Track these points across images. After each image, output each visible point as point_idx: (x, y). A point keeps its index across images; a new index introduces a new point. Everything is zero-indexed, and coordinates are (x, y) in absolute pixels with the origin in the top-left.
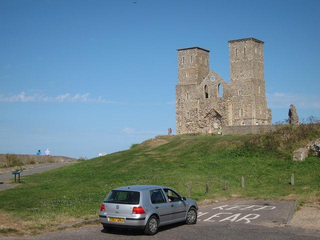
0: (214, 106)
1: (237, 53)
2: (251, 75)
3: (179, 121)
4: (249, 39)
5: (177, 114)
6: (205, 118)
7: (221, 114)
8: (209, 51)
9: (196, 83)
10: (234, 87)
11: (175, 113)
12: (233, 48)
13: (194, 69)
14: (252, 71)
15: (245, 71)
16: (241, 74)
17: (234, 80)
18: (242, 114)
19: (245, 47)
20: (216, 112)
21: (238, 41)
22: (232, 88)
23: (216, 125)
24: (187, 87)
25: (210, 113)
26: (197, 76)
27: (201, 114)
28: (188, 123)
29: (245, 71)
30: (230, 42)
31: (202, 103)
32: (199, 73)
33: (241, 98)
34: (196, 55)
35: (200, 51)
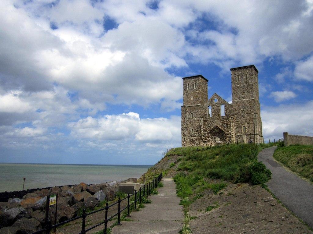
1: (238, 78)
2: (253, 97)
6: (208, 133)
7: (224, 130)
8: (207, 81)
9: (200, 104)
10: (236, 107)
13: (199, 93)
17: (236, 101)
18: (245, 130)
19: (247, 73)
22: (234, 108)
23: (218, 140)
24: (192, 108)
25: (213, 130)
26: (200, 98)
27: (205, 130)
28: (193, 138)
29: (247, 94)
31: (205, 121)
32: (202, 97)
33: (243, 116)
34: (199, 81)
35: (203, 80)
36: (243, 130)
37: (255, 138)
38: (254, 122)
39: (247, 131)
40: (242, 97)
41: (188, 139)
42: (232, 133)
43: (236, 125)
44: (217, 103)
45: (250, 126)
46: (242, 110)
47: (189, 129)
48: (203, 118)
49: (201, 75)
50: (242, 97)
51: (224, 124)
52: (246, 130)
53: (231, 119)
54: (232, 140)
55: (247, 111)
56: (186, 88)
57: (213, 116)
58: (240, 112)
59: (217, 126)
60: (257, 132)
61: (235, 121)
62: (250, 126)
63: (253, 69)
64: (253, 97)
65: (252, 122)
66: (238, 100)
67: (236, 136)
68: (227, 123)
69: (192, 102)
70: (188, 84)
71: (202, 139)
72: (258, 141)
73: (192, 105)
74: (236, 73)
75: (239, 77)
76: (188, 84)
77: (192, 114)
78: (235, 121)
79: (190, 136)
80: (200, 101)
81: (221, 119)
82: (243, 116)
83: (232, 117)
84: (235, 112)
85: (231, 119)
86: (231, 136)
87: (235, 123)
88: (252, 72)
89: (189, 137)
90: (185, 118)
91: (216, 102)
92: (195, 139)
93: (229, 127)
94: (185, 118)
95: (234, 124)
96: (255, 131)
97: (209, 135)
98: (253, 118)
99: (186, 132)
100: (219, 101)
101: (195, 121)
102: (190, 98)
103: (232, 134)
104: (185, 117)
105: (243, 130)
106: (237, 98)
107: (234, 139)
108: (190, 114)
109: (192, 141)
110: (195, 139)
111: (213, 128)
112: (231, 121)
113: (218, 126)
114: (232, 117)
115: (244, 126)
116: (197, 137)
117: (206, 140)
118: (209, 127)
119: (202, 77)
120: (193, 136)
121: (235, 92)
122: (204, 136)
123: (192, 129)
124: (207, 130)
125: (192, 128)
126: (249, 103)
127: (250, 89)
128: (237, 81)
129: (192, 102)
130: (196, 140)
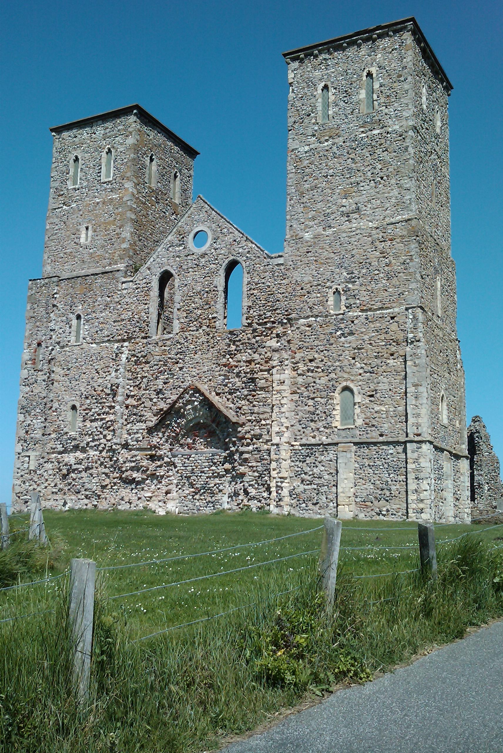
0: (202, 373)
1: (326, 106)
3: (26, 441)
4: (396, 28)
5: (25, 410)
6: (150, 431)
9: (121, 266)
10: (303, 275)
11: (16, 407)
12: (311, 84)
13: (121, 202)
14: (407, 183)
15: (367, 188)
16: (349, 204)
18: (347, 416)
19: (374, 70)
20: (207, 403)
21: (335, 45)
22: (296, 276)
26: (127, 232)
29: (367, 188)
30: (294, 56)
31: (138, 360)
33: (344, 327)
34: (131, 141)
36: (337, 413)
37: (410, 466)
38: (405, 362)
39: (359, 422)
40: (343, 214)
41: (49, 466)
42: (275, 428)
43: (300, 380)
44: (203, 255)
45: (381, 386)
46: (340, 288)
47: (56, 405)
48: (129, 339)
49: (137, 107)
50: (343, 214)
51: (238, 375)
52: (357, 410)
53: (273, 343)
54: (274, 474)
55: (364, 296)
56: (64, 182)
57: (183, 330)
58: (323, 303)
59: (197, 390)
60: (418, 426)
61: (298, 356)
62: (381, 386)
63: (408, 38)
64: (406, 208)
65: (391, 362)
66: (320, 229)
67: (295, 452)
68: (252, 372)
69: (86, 258)
70: (76, 160)
71: (116, 467)
72: (424, 485)
73: (83, 272)
74: (317, 73)
75: (332, 98)
76: (76, 160)
77: (79, 317)
78: (298, 356)
79: (60, 448)
80: (124, 246)
81: (222, 346)
82: (344, 327)
83: (280, 330)
84: (296, 303)
85: (273, 343)
86: (269, 451)
87: (295, 369)
88: (402, 59)
89: (53, 450)
90: (39, 345)
91: (203, 249)
92: (81, 467)
93: (262, 394)
94: (39, 345)
95: (288, 372)
96: (411, 420)
97: (155, 440)
98: (400, 336)
99: (38, 423)
100: (216, 239)
101: (90, 358)
102: (76, 233)
103: (276, 440)
104: (41, 337)
105: (337, 413)
106: (313, 219)
107: (283, 466)
108: (68, 322)
109: (67, 473)
110: (81, 467)
111: (174, 397)
112: (276, 356)
113: (204, 388)
114: (280, 330)
115: (346, 389)
116: (92, 453)
117: (136, 469)
118: (159, 392)
119: (146, 118)
120: (76, 448)
121: (307, 186)
122: (126, 446)
123: (74, 408)
124: (148, 415)
125: (70, 399)
126: (380, 246)
127: (386, 164)
128: (320, 121)
129: (86, 258)
130: (87, 469)
